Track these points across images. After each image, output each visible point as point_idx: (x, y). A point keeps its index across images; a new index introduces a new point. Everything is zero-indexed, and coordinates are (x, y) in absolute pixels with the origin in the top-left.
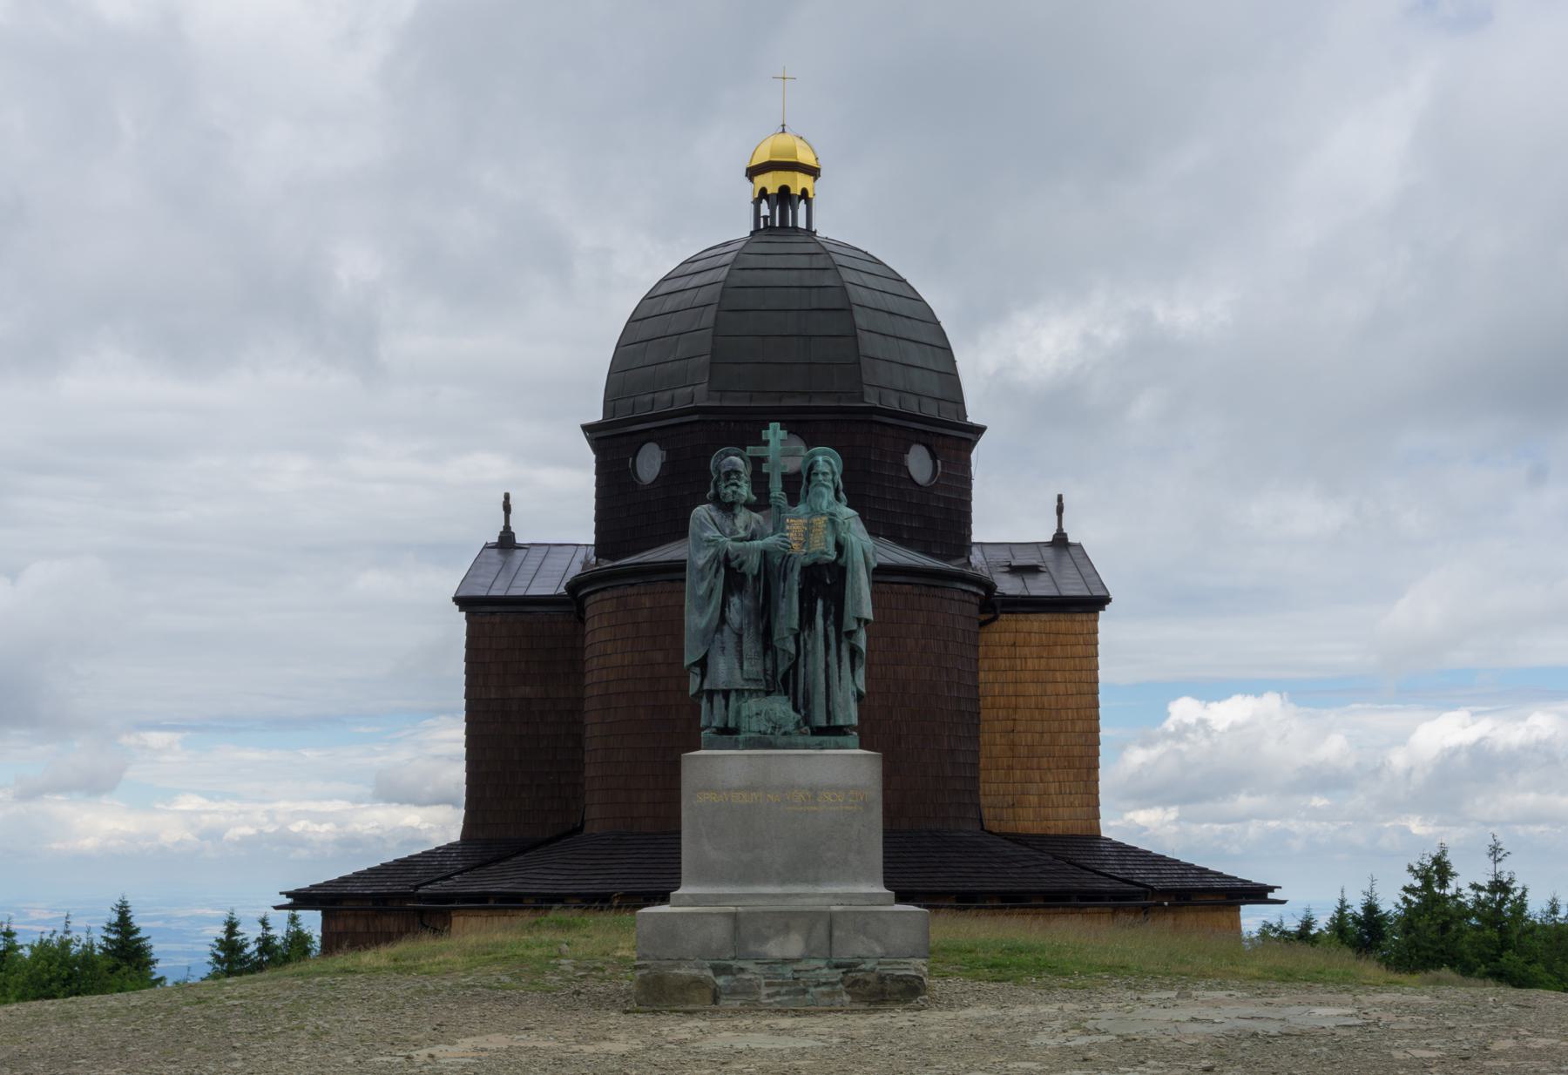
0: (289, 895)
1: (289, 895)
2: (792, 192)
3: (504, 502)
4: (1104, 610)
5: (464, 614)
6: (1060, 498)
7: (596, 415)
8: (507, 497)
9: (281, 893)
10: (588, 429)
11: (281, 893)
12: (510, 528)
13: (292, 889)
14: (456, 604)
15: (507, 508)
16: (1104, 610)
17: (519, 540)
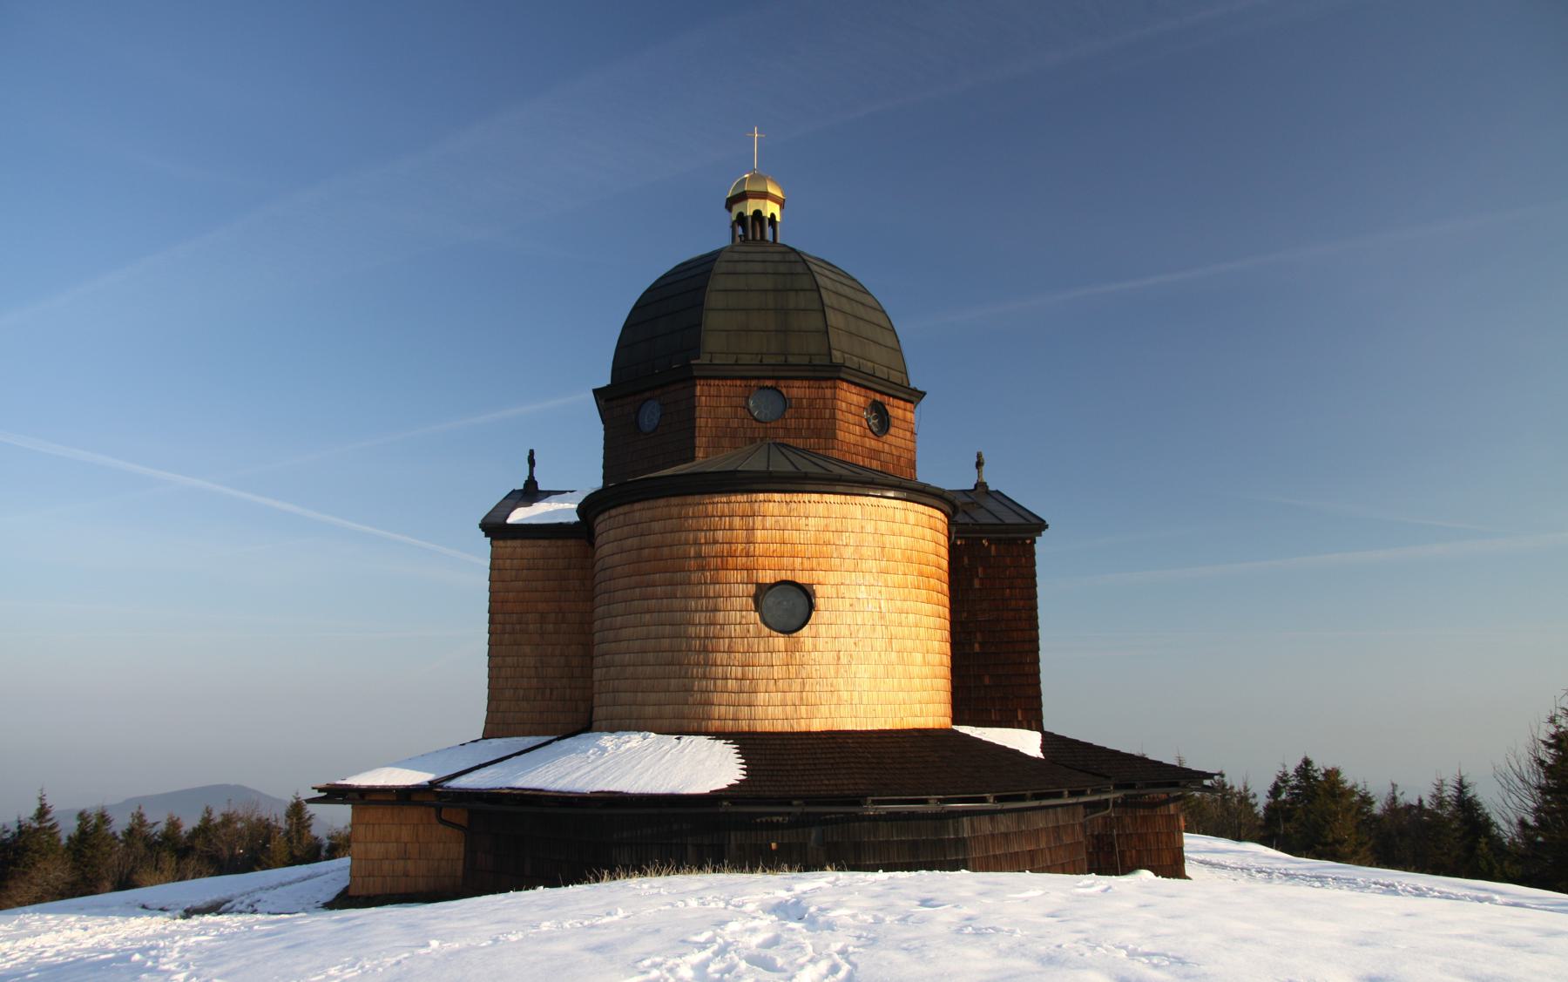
0: (320, 790)
1: (320, 790)
2: (764, 215)
3: (529, 457)
4: (1041, 535)
5: (489, 539)
6: (979, 456)
7: (605, 380)
8: (532, 453)
9: (313, 788)
10: (596, 392)
11: (313, 788)
12: (534, 478)
13: (322, 784)
14: (483, 530)
15: (532, 462)
16: (1041, 535)
17: (541, 487)
